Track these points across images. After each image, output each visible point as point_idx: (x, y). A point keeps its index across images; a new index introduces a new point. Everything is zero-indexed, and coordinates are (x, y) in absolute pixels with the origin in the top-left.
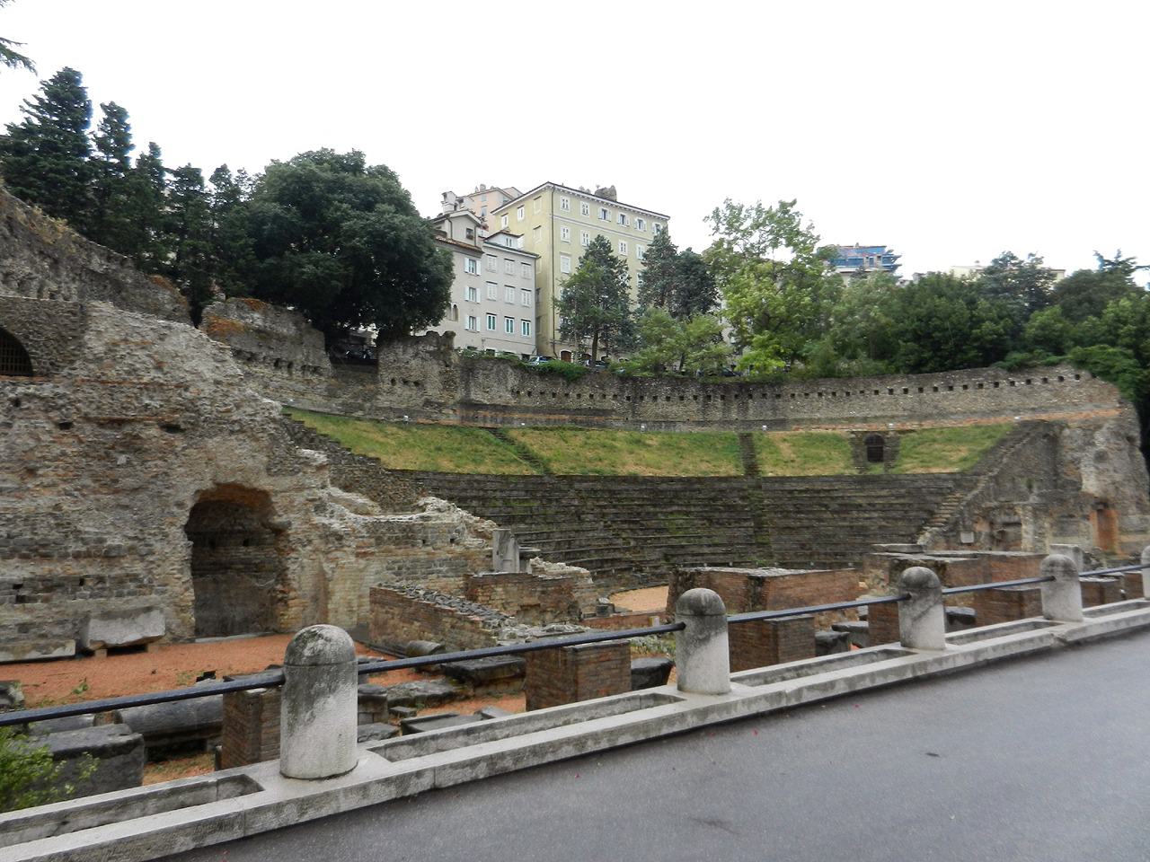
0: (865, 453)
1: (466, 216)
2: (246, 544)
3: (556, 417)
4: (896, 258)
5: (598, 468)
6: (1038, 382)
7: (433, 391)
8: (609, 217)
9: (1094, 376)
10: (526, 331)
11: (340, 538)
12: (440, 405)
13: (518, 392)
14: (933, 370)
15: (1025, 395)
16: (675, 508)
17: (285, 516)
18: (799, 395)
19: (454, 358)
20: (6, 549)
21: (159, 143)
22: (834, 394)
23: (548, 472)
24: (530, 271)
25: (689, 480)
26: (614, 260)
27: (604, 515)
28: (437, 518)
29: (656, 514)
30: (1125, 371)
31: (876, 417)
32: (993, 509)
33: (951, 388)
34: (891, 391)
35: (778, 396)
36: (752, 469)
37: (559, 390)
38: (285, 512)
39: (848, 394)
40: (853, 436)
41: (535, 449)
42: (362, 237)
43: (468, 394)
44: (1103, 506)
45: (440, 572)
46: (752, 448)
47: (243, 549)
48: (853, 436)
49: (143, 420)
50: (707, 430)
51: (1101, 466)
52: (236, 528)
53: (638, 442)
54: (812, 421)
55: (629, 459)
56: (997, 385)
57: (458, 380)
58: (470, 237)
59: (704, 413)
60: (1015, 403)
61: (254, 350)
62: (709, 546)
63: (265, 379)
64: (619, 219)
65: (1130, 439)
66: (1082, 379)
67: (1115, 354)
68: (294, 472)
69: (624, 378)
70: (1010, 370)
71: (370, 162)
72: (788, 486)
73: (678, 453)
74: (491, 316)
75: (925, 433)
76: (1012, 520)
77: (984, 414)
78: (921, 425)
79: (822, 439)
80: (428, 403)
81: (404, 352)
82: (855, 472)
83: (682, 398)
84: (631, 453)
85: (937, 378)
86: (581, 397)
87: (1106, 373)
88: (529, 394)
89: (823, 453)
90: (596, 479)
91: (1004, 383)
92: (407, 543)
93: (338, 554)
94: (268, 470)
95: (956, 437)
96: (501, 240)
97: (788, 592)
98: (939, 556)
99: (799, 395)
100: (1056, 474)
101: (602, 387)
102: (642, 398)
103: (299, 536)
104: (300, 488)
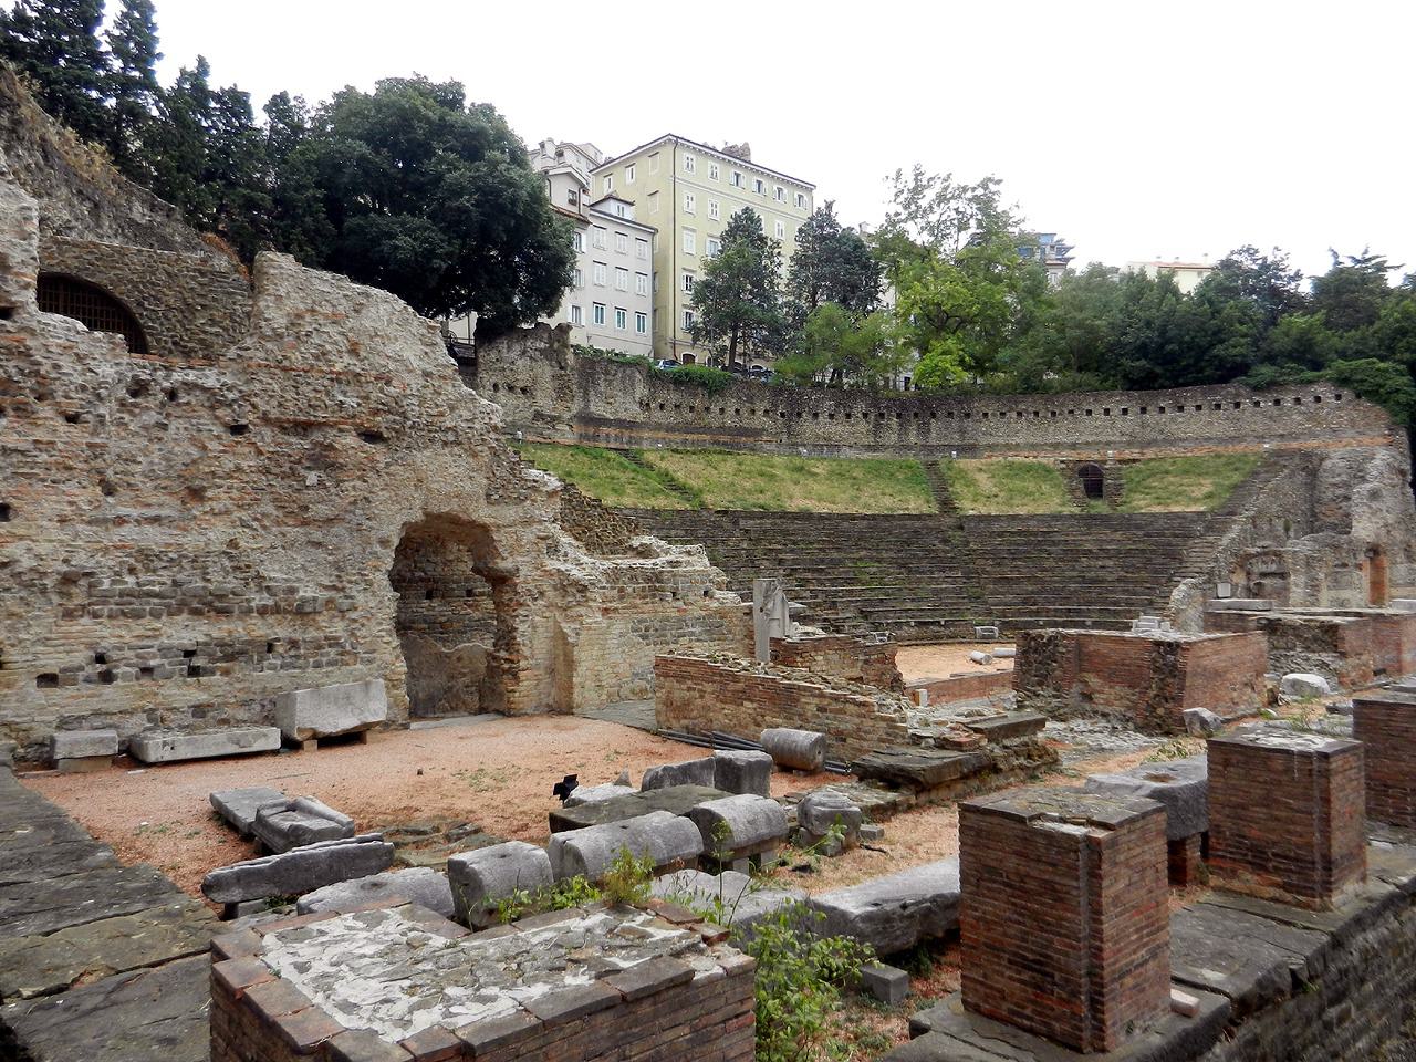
0: (1082, 486)
1: (569, 174)
2: (429, 596)
3: (695, 437)
4: (1068, 249)
5: (761, 502)
6: (1288, 402)
7: (545, 401)
8: (742, 182)
9: (1358, 396)
10: (641, 327)
11: (583, 589)
12: (555, 419)
13: (648, 405)
14: (1162, 387)
15: (1271, 418)
16: (863, 553)
17: (510, 560)
18: (994, 415)
19: (570, 358)
20: (173, 601)
21: (208, 60)
22: (1036, 414)
23: (704, 506)
24: (647, 248)
25: (874, 517)
26: (762, 239)
27: (781, 562)
28: (688, 563)
29: (840, 561)
30: (1397, 391)
31: (1087, 443)
32: (1254, 556)
33: (1181, 409)
34: (1107, 412)
35: (968, 415)
36: (947, 505)
37: (697, 403)
38: (511, 554)
39: (1054, 414)
40: (1064, 466)
41: (680, 476)
42: (471, 195)
43: (587, 406)
44: (1375, 551)
45: (693, 634)
46: (941, 477)
47: (426, 603)
48: (1064, 466)
49: (336, 423)
50: (879, 455)
51: (1374, 505)
52: (417, 574)
53: (800, 469)
54: (1008, 447)
55: (796, 490)
56: (1237, 405)
57: (575, 387)
58: (572, 202)
59: (875, 433)
60: (1260, 429)
62: (913, 600)
64: (755, 188)
65: (1402, 473)
66: (1343, 399)
67: (1386, 370)
68: (520, 500)
69: (778, 390)
70: (1257, 389)
71: (472, 98)
72: (996, 527)
73: (853, 485)
74: (599, 307)
75: (1152, 463)
76: (1269, 570)
77: (1221, 441)
78: (1143, 454)
79: (1029, 469)
80: (538, 416)
81: (509, 348)
82: (1076, 510)
83: (848, 416)
84: (797, 483)
85: (1165, 395)
86: (727, 412)
87: (1373, 393)
88: (662, 406)
89: (1032, 486)
90: (762, 516)
91: (1246, 404)
92: (654, 596)
93: (582, 610)
94: (488, 496)
95: (1193, 469)
96: (612, 207)
97: (1205, 662)
98: (1320, 614)
99: (994, 415)
100: (1314, 515)
101: (751, 400)
102: (799, 415)
103: (529, 587)
104: (528, 522)
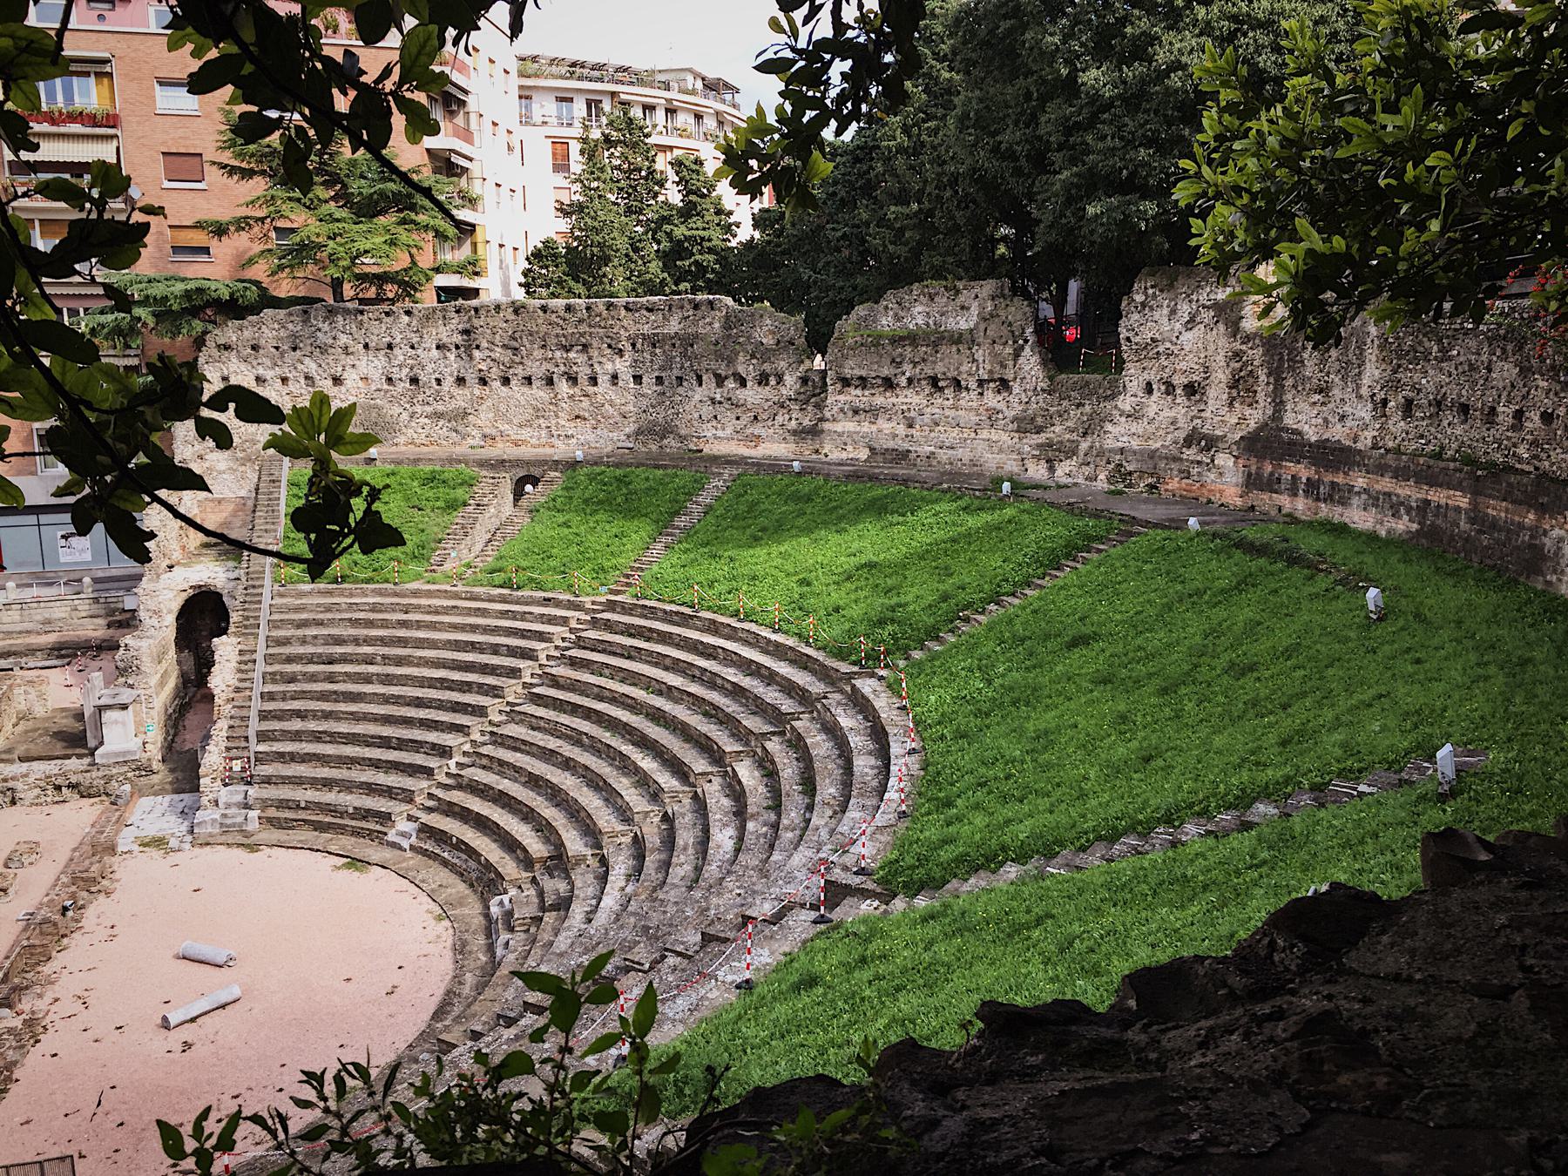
13: (1385, 402)
61: (886, 371)
63: (913, 414)
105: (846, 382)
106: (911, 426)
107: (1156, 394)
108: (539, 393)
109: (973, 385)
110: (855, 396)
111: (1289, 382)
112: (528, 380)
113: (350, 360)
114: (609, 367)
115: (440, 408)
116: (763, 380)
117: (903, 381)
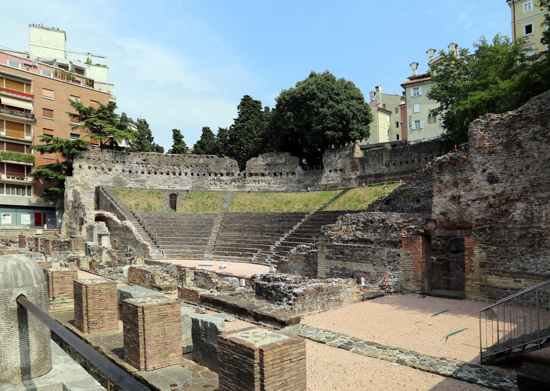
3: (406, 175)
13: (389, 165)
61: (262, 172)
81: (335, 156)
88: (394, 164)
105: (251, 175)
106: (269, 184)
107: (332, 172)
108: (165, 176)
109: (285, 174)
110: (254, 178)
111: (366, 165)
112: (162, 174)
113: (114, 165)
114: (185, 171)
115: (138, 179)
116: (228, 174)
117: (267, 174)
